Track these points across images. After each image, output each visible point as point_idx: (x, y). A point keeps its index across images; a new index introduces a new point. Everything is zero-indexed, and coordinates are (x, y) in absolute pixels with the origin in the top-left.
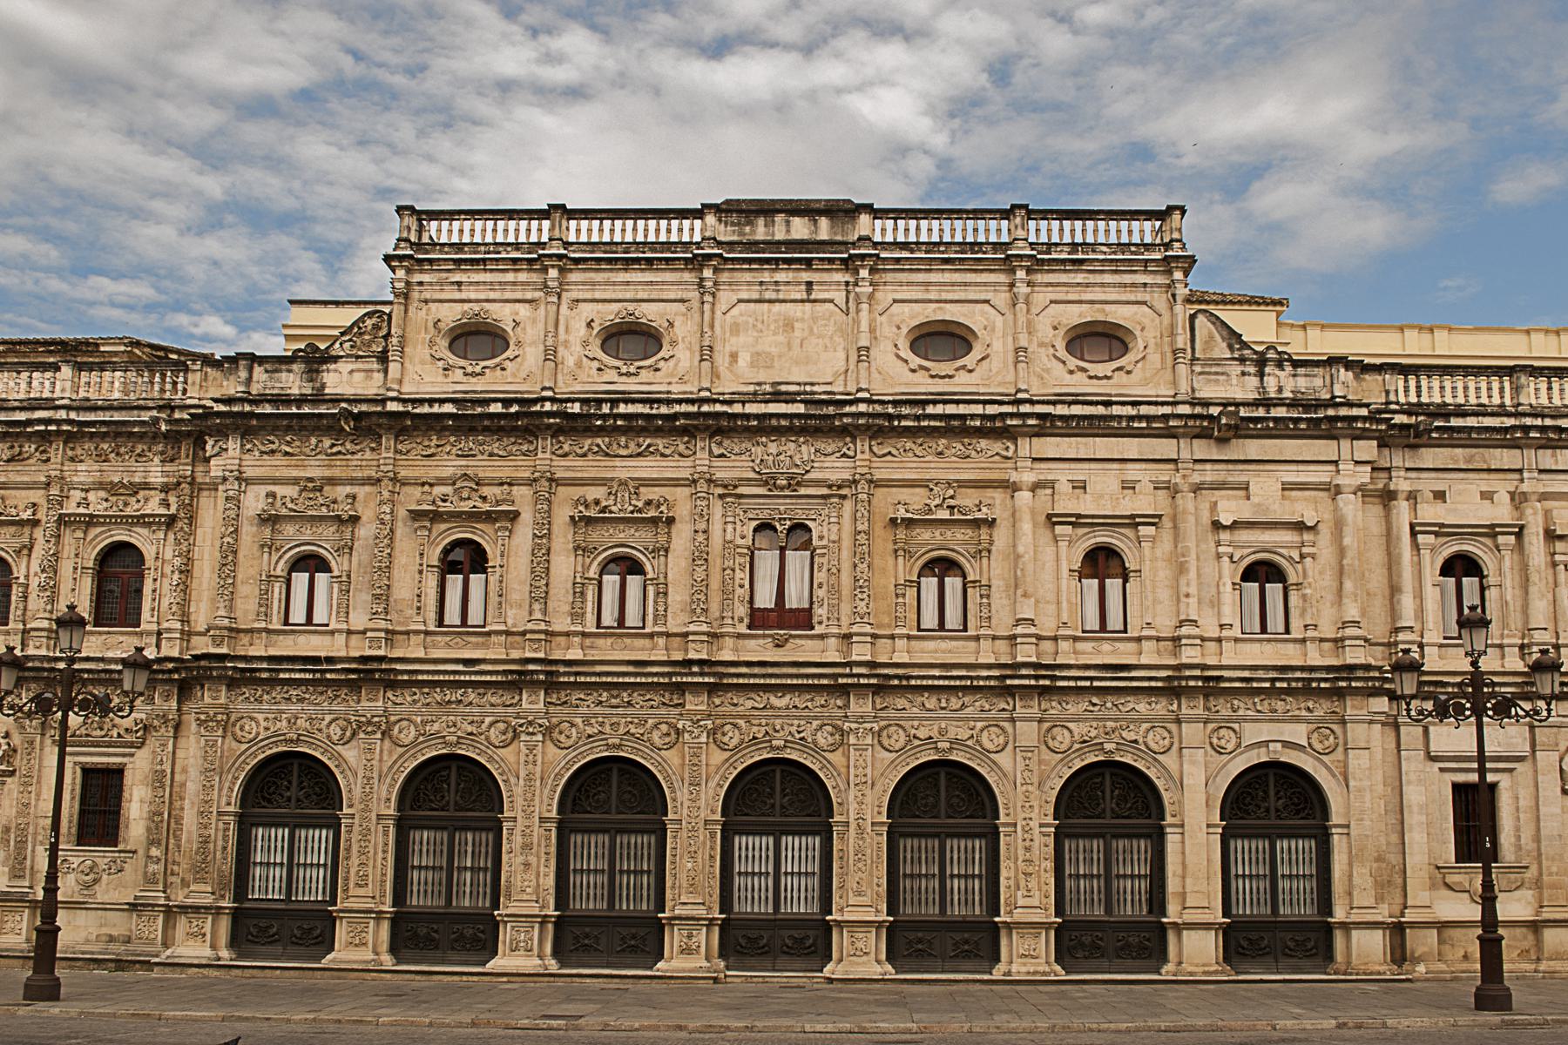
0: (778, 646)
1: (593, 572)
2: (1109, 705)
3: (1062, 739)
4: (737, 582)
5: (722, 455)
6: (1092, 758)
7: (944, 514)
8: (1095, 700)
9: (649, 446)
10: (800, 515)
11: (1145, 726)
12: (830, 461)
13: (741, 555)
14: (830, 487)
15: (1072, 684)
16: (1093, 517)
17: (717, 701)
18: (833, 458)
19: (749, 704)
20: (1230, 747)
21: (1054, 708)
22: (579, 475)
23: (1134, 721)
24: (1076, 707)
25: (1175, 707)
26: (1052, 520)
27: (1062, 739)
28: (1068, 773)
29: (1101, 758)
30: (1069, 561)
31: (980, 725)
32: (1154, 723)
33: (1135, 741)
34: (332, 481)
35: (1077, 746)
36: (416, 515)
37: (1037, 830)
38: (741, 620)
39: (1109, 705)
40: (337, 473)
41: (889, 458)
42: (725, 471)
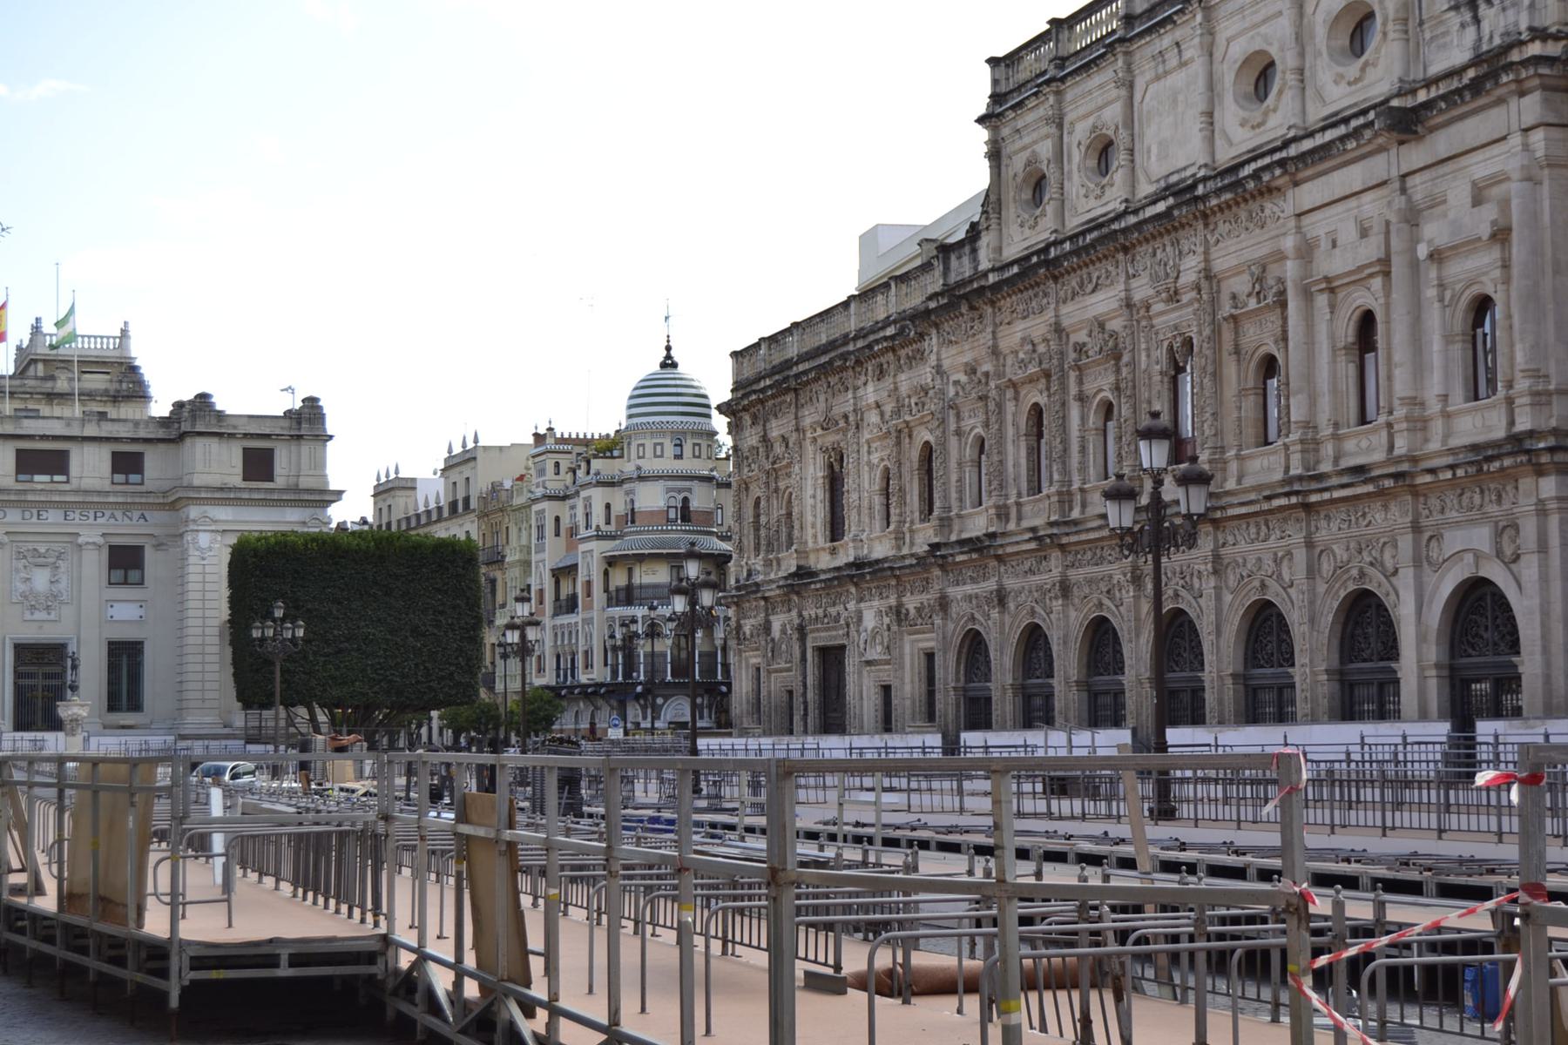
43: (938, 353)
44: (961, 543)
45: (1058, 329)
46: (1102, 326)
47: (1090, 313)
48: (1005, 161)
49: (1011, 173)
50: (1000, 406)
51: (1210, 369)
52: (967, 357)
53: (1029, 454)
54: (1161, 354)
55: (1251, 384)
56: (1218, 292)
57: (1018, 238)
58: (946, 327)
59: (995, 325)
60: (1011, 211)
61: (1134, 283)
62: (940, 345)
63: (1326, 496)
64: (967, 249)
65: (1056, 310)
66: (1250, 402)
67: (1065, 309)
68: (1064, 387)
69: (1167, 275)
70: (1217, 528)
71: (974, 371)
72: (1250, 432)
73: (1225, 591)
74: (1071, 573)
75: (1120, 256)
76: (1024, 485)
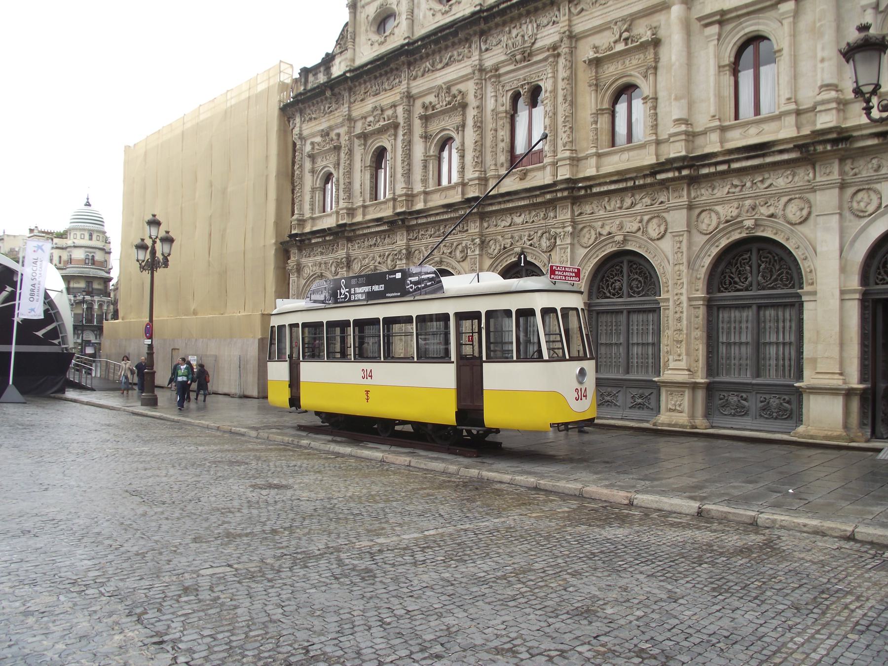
0: (521, 179)
1: (432, 151)
2: (748, 184)
3: (709, 222)
4: (500, 138)
5: (487, 50)
6: (736, 236)
7: (620, 47)
8: (736, 182)
9: (450, 58)
10: (534, 79)
11: (784, 200)
12: (546, 31)
13: (501, 118)
14: (548, 50)
15: (712, 170)
16: (736, 9)
17: (485, 225)
18: (549, 27)
19: (503, 224)
20: (871, 209)
21: (704, 194)
22: (421, 89)
23: (772, 196)
24: (722, 190)
25: (811, 175)
26: (707, 21)
27: (709, 222)
28: (715, 251)
29: (744, 235)
30: (718, 56)
31: (646, 218)
32: (791, 195)
33: (772, 216)
34: (331, 128)
35: (722, 226)
36: (359, 137)
37: (685, 305)
38: (502, 165)
39: (748, 184)
40: (332, 123)
41: (583, 13)
42: (490, 61)
43: (300, 127)
44: (314, 233)
45: (410, 97)
46: (449, 88)
47: (439, 82)
48: (359, 9)
49: (363, 16)
50: (350, 153)
51: (569, 98)
52: (323, 124)
53: (371, 178)
54: (506, 99)
55: (606, 105)
56: (576, 48)
57: (366, 51)
58: (308, 111)
59: (350, 103)
60: (362, 39)
61: (486, 55)
62: (302, 122)
63: (712, 170)
64: (322, 69)
65: (408, 84)
66: (604, 120)
67: (413, 84)
68: (409, 131)
69: (524, 42)
70: (573, 204)
71: (328, 134)
72: (605, 138)
73: (577, 246)
74: (412, 243)
75: (476, 39)
76: (368, 196)
